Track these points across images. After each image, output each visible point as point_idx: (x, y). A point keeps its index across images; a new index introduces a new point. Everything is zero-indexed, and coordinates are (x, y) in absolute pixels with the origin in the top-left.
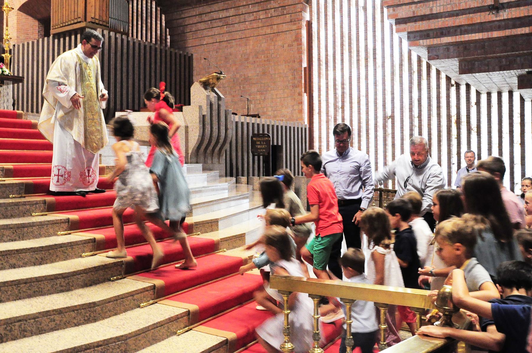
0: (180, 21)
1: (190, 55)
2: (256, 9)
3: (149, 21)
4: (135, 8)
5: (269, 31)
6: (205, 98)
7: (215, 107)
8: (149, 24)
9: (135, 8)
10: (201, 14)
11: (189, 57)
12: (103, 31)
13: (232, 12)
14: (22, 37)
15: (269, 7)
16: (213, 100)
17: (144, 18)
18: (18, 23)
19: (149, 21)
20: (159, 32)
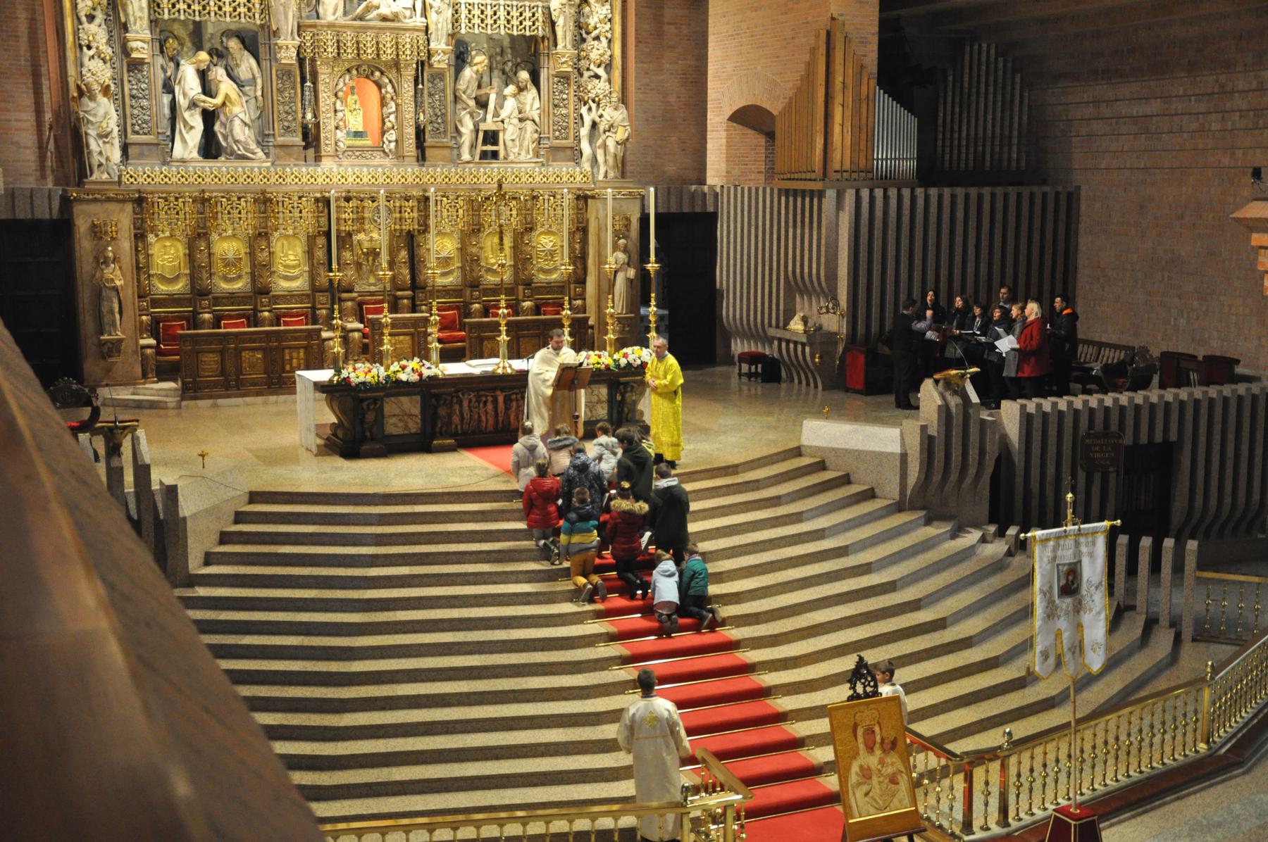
0: (1060, 108)
1: (1071, 189)
2: (1202, 107)
3: (1009, 88)
4: (984, 54)
5: (1226, 161)
6: (936, 408)
7: (957, 421)
8: (1008, 96)
9: (984, 54)
10: (1096, 102)
11: (1070, 195)
12: (858, 191)
13: (1154, 107)
14: (736, 172)
15: (1228, 105)
16: (954, 410)
17: (1000, 81)
18: (729, 145)
19: (1009, 88)
20: (1025, 118)
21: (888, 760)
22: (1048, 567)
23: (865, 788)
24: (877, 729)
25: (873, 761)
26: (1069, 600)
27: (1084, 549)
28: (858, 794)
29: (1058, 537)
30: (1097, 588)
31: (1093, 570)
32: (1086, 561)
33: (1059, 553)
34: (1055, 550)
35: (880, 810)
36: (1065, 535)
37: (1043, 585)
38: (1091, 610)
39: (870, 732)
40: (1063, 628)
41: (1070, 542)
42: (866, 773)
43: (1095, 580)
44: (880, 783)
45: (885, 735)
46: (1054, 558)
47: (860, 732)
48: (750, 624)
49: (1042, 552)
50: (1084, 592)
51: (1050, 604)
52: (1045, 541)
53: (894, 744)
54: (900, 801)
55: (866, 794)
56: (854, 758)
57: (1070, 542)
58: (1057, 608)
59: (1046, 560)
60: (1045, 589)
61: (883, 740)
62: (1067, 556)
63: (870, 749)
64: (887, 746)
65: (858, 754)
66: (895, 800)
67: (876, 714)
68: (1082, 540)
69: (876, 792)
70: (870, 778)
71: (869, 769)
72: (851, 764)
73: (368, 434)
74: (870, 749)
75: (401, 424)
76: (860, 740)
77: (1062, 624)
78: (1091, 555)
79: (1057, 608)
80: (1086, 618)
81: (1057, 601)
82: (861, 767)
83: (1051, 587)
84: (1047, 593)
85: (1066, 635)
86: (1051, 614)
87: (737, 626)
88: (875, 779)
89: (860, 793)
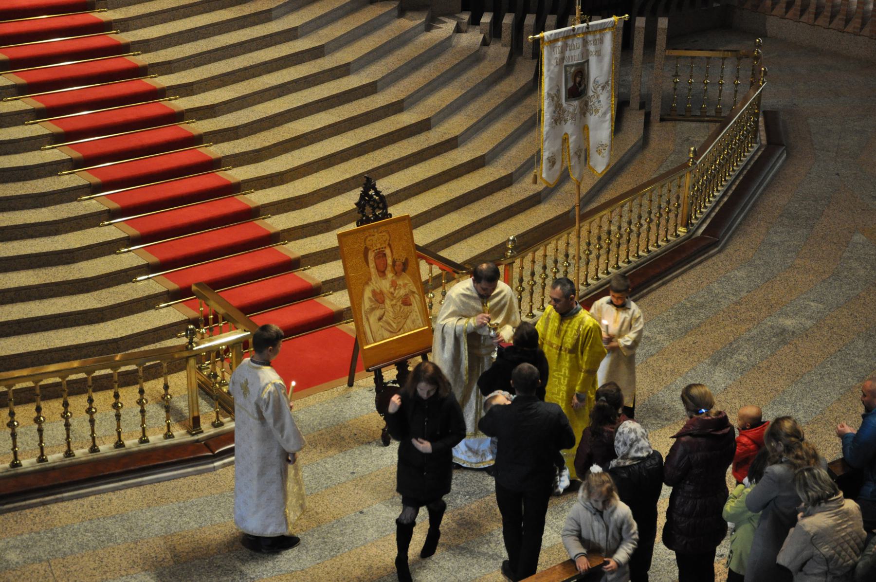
21: (400, 282)
22: (556, 70)
23: (378, 313)
24: (388, 251)
25: (385, 285)
26: (576, 103)
27: (592, 48)
29: (566, 37)
30: (603, 88)
31: (600, 70)
32: (593, 60)
33: (567, 54)
34: (562, 52)
35: (393, 333)
36: (574, 34)
37: (551, 89)
38: (597, 111)
40: (569, 133)
41: (578, 41)
42: (379, 298)
43: (602, 80)
44: (393, 306)
45: (396, 257)
46: (562, 59)
47: (371, 256)
48: (229, 140)
49: (550, 54)
50: (591, 93)
51: (558, 109)
52: (553, 41)
53: (405, 266)
54: (413, 322)
55: (380, 319)
56: (367, 283)
57: (578, 41)
58: (564, 111)
59: (554, 62)
60: (553, 92)
61: (394, 262)
62: (574, 56)
63: (382, 273)
64: (399, 268)
65: (370, 279)
66: (409, 321)
67: (387, 236)
68: (590, 38)
69: (389, 315)
70: (383, 302)
71: (382, 293)
72: (363, 290)
74: (382, 273)
76: (372, 265)
77: (569, 128)
78: (599, 53)
79: (564, 111)
80: (592, 120)
81: (564, 105)
82: (374, 292)
83: (559, 91)
84: (554, 98)
85: (572, 139)
86: (558, 120)
87: (216, 143)
88: (388, 302)
89: (373, 318)
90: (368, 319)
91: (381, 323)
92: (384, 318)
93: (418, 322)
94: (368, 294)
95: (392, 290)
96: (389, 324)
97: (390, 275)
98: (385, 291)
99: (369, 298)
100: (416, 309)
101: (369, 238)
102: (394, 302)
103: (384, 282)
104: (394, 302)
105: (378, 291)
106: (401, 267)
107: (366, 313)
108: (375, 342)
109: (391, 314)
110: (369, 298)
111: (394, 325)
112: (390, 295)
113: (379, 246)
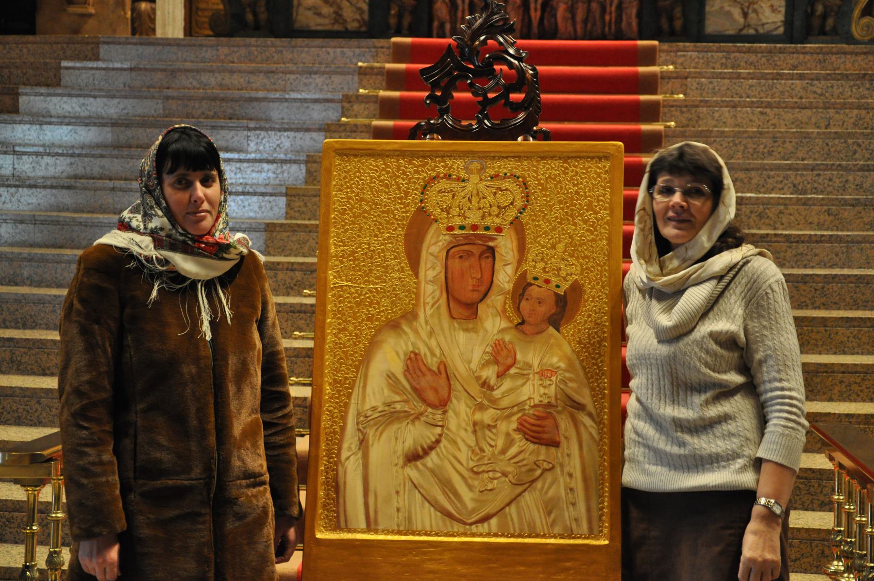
21: (531, 355)
23: (413, 435)
24: (506, 245)
28: (378, 451)
39: (475, 249)
42: (428, 387)
45: (534, 268)
47: (435, 244)
55: (414, 457)
56: (394, 326)
61: (522, 287)
63: (465, 307)
64: (538, 306)
65: (411, 316)
70: (443, 404)
71: (444, 371)
72: (373, 345)
73: (250, 17)
75: (326, 10)
88: (461, 411)
90: (363, 444)
91: (411, 472)
92: (432, 459)
93: (568, 514)
94: (389, 358)
95: (490, 373)
96: (447, 486)
97: (493, 323)
98: (460, 368)
99: (390, 376)
100: (575, 465)
101: (443, 184)
102: (487, 416)
103: (462, 337)
104: (487, 416)
105: (432, 362)
106: (543, 310)
107: (364, 420)
108: (369, 529)
109: (464, 454)
110: (390, 376)
111: (467, 495)
112: (475, 389)
113: (474, 218)
